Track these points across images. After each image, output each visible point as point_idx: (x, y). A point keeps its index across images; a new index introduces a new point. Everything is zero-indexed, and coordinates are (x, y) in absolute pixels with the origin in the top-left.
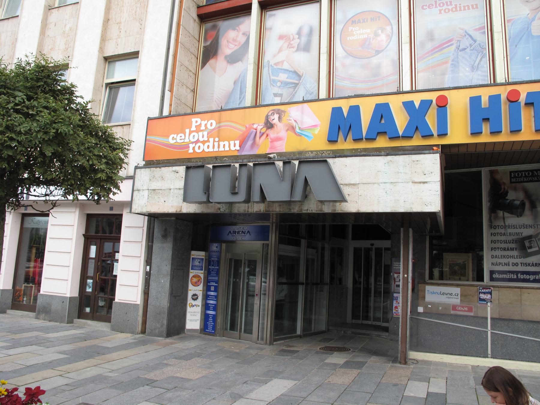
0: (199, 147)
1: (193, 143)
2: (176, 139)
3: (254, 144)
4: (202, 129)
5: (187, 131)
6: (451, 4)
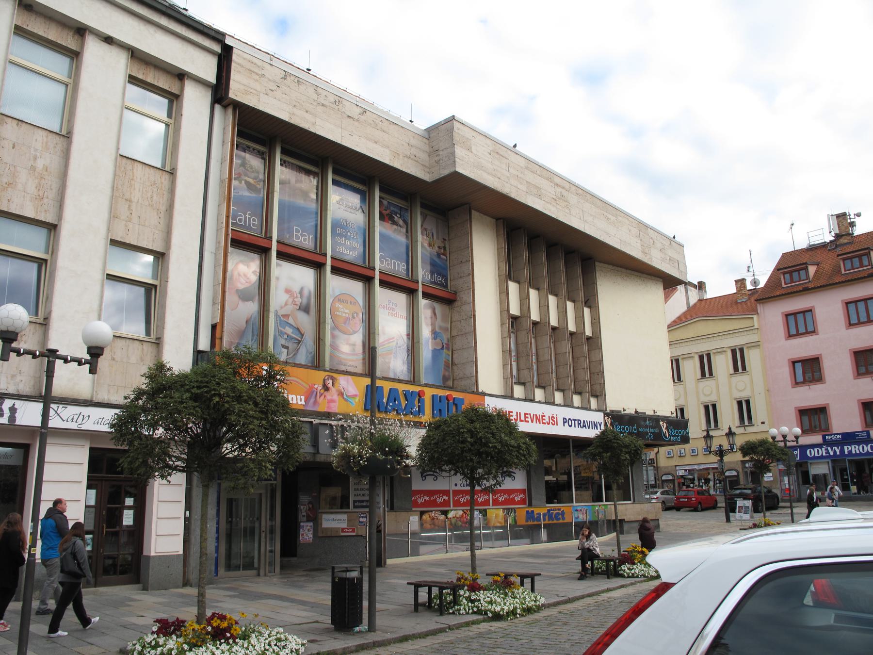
3: (315, 402)
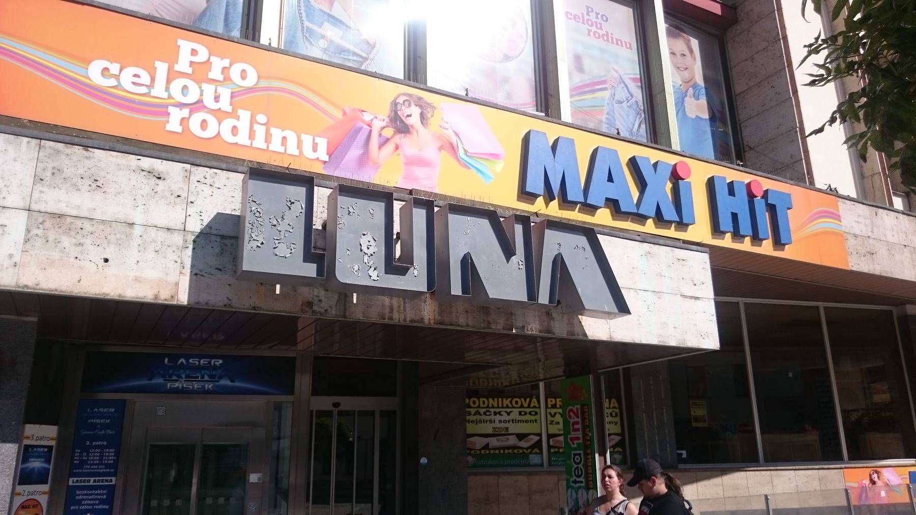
0: (204, 124)
1: (181, 105)
2: (117, 77)
4: (211, 75)
5: (162, 68)
6: (601, 28)
